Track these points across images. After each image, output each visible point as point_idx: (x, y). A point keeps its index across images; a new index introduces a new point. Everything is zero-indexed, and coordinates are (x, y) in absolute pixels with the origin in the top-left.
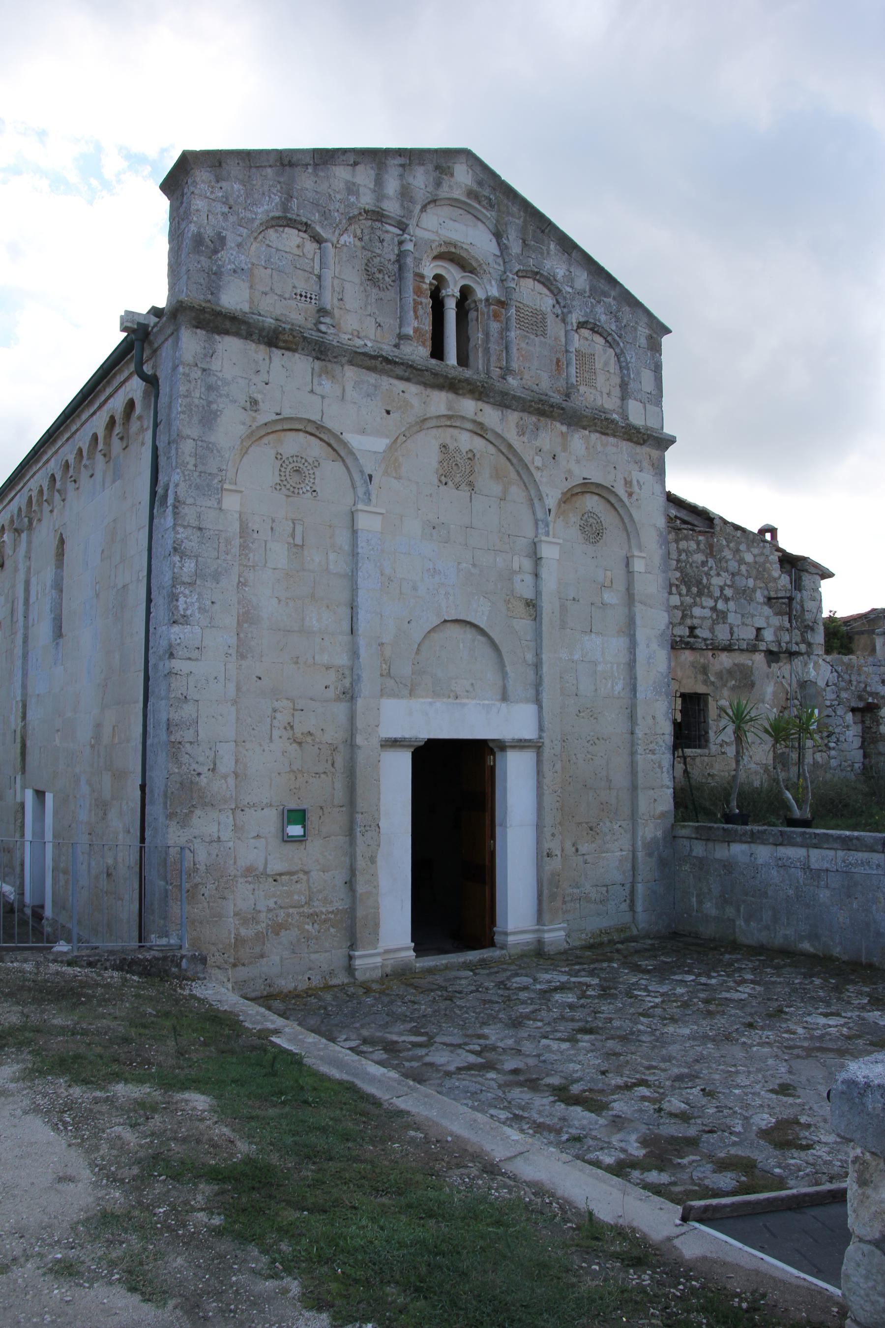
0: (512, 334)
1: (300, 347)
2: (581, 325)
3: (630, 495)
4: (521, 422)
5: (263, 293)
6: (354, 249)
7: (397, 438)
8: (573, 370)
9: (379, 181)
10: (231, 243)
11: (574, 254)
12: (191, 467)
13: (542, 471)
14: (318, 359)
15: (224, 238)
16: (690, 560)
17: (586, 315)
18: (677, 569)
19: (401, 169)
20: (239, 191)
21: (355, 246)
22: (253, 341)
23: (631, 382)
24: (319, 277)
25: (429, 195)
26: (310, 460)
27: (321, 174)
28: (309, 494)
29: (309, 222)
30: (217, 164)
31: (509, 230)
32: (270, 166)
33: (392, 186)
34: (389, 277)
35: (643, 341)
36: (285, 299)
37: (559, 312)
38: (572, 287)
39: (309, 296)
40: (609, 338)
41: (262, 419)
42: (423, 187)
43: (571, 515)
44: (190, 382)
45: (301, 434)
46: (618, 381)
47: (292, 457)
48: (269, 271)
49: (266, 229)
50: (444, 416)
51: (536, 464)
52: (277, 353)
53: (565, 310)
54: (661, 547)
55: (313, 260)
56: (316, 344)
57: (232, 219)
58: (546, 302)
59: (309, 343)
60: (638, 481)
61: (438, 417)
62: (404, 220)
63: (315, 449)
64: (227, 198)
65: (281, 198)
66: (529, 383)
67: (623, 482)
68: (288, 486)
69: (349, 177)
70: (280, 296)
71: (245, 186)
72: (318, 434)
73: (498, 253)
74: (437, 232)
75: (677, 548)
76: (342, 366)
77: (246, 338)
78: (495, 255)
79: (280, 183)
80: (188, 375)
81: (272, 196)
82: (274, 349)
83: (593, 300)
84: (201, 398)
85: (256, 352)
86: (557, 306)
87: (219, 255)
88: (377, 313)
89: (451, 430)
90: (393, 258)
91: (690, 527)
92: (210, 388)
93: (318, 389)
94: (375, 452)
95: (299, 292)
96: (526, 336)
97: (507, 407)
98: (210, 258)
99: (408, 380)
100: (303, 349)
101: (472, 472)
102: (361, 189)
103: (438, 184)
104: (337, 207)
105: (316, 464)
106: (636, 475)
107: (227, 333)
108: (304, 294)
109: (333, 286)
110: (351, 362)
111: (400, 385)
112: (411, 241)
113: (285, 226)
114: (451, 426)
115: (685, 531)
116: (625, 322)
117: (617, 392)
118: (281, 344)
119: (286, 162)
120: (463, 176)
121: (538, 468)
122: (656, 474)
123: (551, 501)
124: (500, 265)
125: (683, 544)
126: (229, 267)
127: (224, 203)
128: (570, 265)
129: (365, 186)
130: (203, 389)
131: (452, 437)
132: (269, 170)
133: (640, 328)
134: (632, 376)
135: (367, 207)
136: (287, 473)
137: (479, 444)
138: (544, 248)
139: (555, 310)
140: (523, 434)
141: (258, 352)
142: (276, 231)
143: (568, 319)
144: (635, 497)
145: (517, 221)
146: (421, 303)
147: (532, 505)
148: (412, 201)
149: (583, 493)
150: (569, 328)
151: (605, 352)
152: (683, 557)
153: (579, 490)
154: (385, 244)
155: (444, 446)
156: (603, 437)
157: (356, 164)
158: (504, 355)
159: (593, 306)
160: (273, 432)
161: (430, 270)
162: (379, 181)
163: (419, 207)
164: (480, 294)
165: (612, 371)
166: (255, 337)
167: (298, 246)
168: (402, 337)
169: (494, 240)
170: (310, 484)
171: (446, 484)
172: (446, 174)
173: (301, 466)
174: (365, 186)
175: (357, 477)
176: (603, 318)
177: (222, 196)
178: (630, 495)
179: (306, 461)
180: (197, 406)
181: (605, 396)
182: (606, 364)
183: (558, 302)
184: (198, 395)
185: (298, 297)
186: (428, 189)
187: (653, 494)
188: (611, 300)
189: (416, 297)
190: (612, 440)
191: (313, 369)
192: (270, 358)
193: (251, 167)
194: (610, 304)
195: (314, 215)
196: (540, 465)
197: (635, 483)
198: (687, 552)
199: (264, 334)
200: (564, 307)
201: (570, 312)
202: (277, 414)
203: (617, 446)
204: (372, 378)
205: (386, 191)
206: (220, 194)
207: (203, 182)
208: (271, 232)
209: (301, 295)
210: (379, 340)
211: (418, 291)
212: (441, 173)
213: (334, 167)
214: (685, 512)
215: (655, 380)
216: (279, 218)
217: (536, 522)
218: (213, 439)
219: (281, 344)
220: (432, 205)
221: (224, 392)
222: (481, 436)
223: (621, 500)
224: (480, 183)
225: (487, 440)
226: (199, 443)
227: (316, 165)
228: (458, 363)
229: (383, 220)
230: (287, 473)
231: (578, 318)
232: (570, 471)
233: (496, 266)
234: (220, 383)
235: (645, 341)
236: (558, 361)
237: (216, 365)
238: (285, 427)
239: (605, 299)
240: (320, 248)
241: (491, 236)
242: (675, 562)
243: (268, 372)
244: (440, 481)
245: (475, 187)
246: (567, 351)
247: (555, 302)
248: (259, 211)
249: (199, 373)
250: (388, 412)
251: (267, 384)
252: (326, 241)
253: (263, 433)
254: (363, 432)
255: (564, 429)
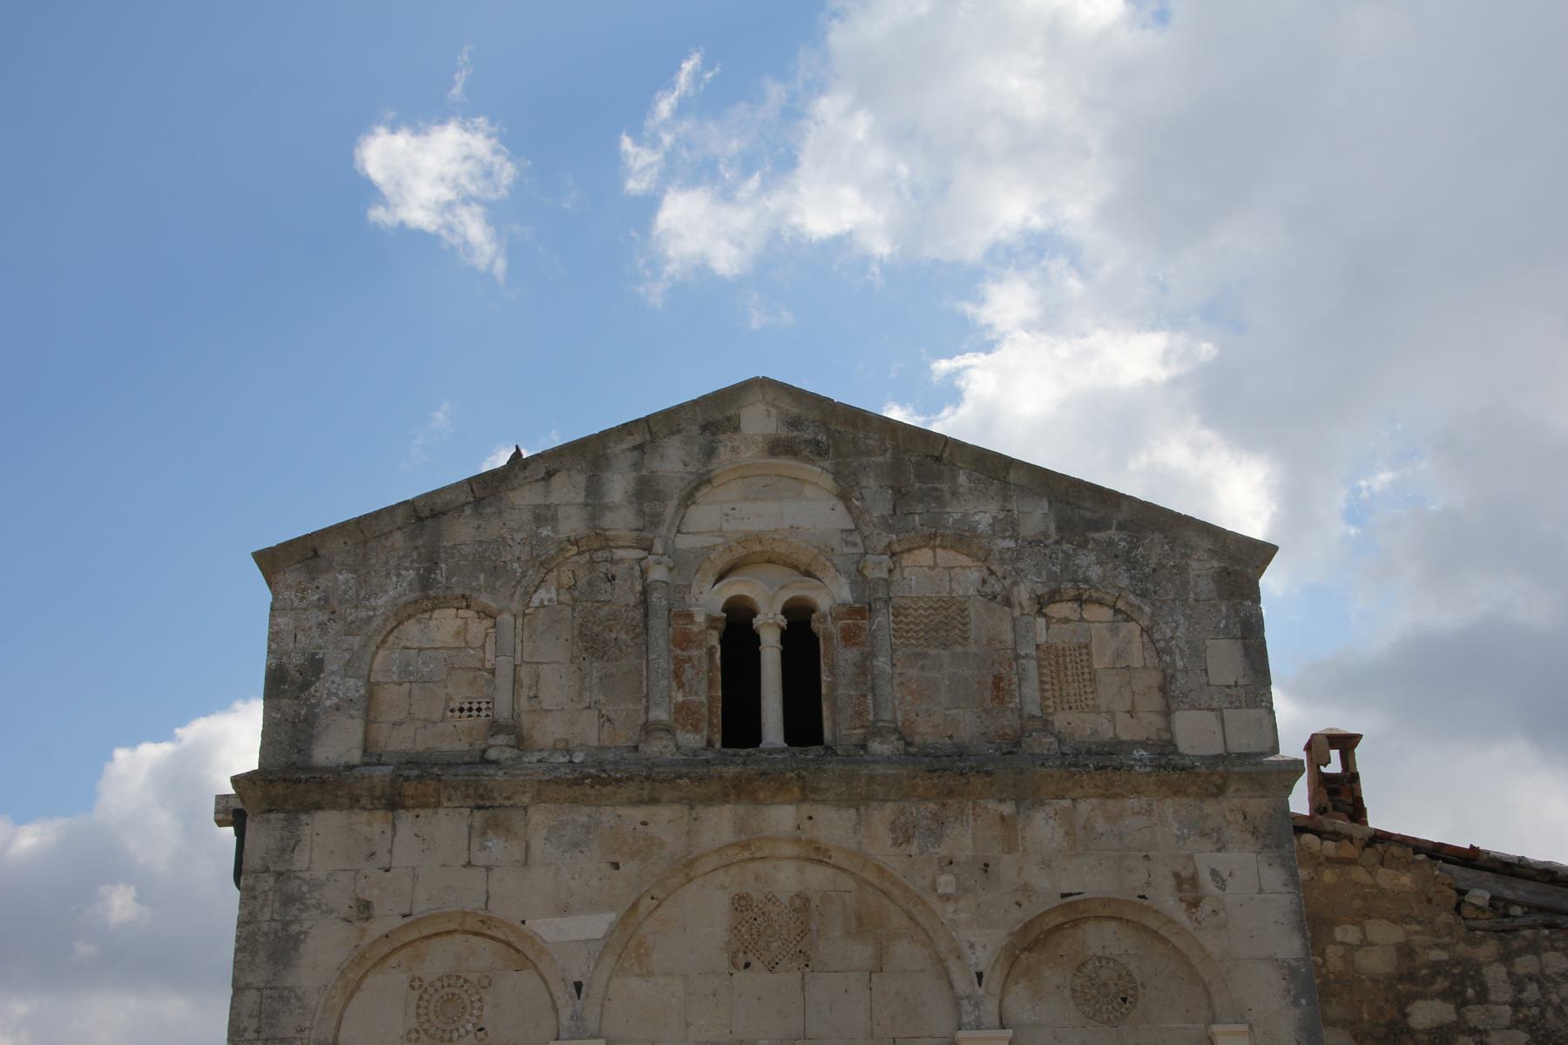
0: (882, 662)
1: (443, 799)
2: (1041, 604)
3: (1194, 904)
4: (902, 819)
5: (394, 724)
6: (558, 607)
7: (635, 906)
8: (1031, 691)
9: (594, 489)
10: (332, 665)
11: (1012, 477)
12: (250, 1035)
13: (957, 900)
14: (479, 808)
15: (322, 660)
16: (1555, 998)
17: (1052, 576)
18: (1515, 1024)
19: (636, 453)
20: (347, 581)
21: (559, 603)
22: (364, 808)
23: (1179, 676)
24: (492, 672)
25: (691, 477)
26: (473, 978)
27: (489, 510)
28: (471, 1036)
29: (467, 593)
30: (311, 554)
31: (864, 482)
32: (399, 529)
33: (618, 485)
34: (627, 633)
35: (1206, 587)
36: (434, 723)
37: (998, 588)
38: (1015, 537)
39: (475, 706)
40: (1120, 605)
41: (376, 929)
42: (680, 467)
43: (1047, 973)
44: (255, 898)
45: (458, 936)
46: (1155, 678)
47: (440, 979)
48: (406, 686)
49: (400, 623)
50: (731, 845)
51: (941, 890)
52: (406, 819)
53: (1007, 582)
54: (1295, 1003)
55: (483, 647)
56: (467, 787)
57: (335, 627)
58: (969, 577)
59: (456, 788)
60: (1214, 873)
61: (718, 851)
62: (646, 534)
63: (483, 955)
64: (326, 600)
65: (418, 570)
66: (930, 739)
67: (1170, 883)
68: (432, 1030)
69: (538, 500)
70: (425, 720)
71: (355, 572)
72: (486, 931)
73: (851, 526)
74: (720, 530)
75: (1509, 974)
76: (525, 808)
77: (351, 807)
78: (843, 531)
79: (416, 548)
80: (253, 888)
81: (403, 572)
82: (401, 812)
83: (1066, 547)
84: (272, 919)
85: (370, 824)
86: (992, 580)
87: (312, 690)
88: (602, 698)
89: (757, 865)
90: (632, 600)
91: (1539, 918)
92: (288, 900)
93: (480, 858)
94: (588, 941)
95: (457, 705)
96: (918, 656)
97: (868, 798)
98: (297, 698)
99: (653, 801)
100: (450, 800)
101: (804, 932)
102: (561, 512)
103: (710, 452)
104: (517, 554)
105: (485, 982)
106: (1206, 860)
107: (319, 807)
108: (466, 706)
109: (516, 680)
110: (539, 798)
111: (640, 813)
112: (659, 563)
113: (432, 610)
114: (752, 860)
115: (1527, 933)
116: (1153, 561)
117: (1156, 701)
118: (410, 802)
119: (426, 513)
120: (758, 422)
121: (946, 898)
122: (1266, 846)
123: (982, 957)
124: (855, 545)
125: (1526, 964)
126: (328, 703)
127: (321, 608)
128: (1006, 498)
129: (568, 504)
130: (277, 905)
131: (757, 878)
132: (398, 535)
133: (1194, 565)
134: (1180, 664)
135: (573, 535)
136: (431, 1008)
137: (817, 878)
138: (945, 487)
139: (988, 589)
140: (908, 840)
141: (371, 824)
142: (419, 621)
143: (1014, 599)
144: (1206, 907)
145: (879, 459)
146: (690, 659)
147: (946, 972)
148: (659, 496)
149: (1075, 923)
150: (1017, 612)
151: (1114, 632)
152: (1531, 992)
153: (1061, 919)
154: (617, 581)
155: (741, 898)
156: (1110, 803)
157: (550, 475)
158: (870, 702)
159: (1067, 556)
160: (405, 945)
161: (709, 600)
162: (594, 489)
163: (672, 504)
164: (823, 602)
165: (1137, 664)
166: (365, 801)
167: (458, 633)
168: (649, 729)
169: (840, 506)
170: (474, 1020)
171: (747, 965)
172: (724, 432)
173: (457, 991)
174: (568, 504)
175: (558, 990)
176: (1095, 573)
177: (319, 599)
178: (1194, 904)
179: (466, 981)
180: (266, 934)
181: (1122, 718)
182: (1119, 655)
183: (992, 573)
184: (268, 917)
185: (457, 714)
186: (689, 469)
187: (1261, 891)
188: (1113, 533)
189: (679, 652)
190: (1133, 803)
191: (471, 827)
192: (394, 827)
193: (366, 542)
194: (1111, 543)
195: (478, 579)
196: (951, 889)
197: (1205, 877)
198: (1541, 979)
199: (378, 793)
200: (1004, 578)
201: (1015, 584)
202: (405, 916)
203: (1149, 813)
204: (582, 815)
205: (607, 500)
206: (316, 597)
207: (288, 587)
208: (411, 628)
209: (461, 710)
210: (607, 743)
211: (684, 640)
212: (714, 434)
213: (511, 494)
214: (1531, 886)
215: (1247, 655)
216: (416, 602)
217: (957, 1002)
218: (290, 981)
219: (410, 802)
220: (704, 490)
221: (313, 901)
222: (821, 861)
223: (1170, 921)
224: (795, 423)
225: (834, 866)
226: (267, 992)
227: (478, 503)
228: (786, 740)
229: (611, 544)
230: (431, 1008)
231: (1033, 590)
232: (1026, 889)
233: (846, 550)
234: (305, 888)
235: (1212, 586)
236: (998, 680)
237: (300, 861)
238: (426, 932)
239: (1097, 536)
240: (494, 626)
241: (835, 501)
242: (1508, 1009)
243: (390, 851)
244: (734, 964)
245: (785, 433)
246: (1017, 657)
247: (986, 572)
248: (380, 602)
249: (271, 880)
250: (616, 866)
251: (387, 871)
252: (500, 612)
253: (386, 950)
254: (564, 910)
255: (1007, 808)
